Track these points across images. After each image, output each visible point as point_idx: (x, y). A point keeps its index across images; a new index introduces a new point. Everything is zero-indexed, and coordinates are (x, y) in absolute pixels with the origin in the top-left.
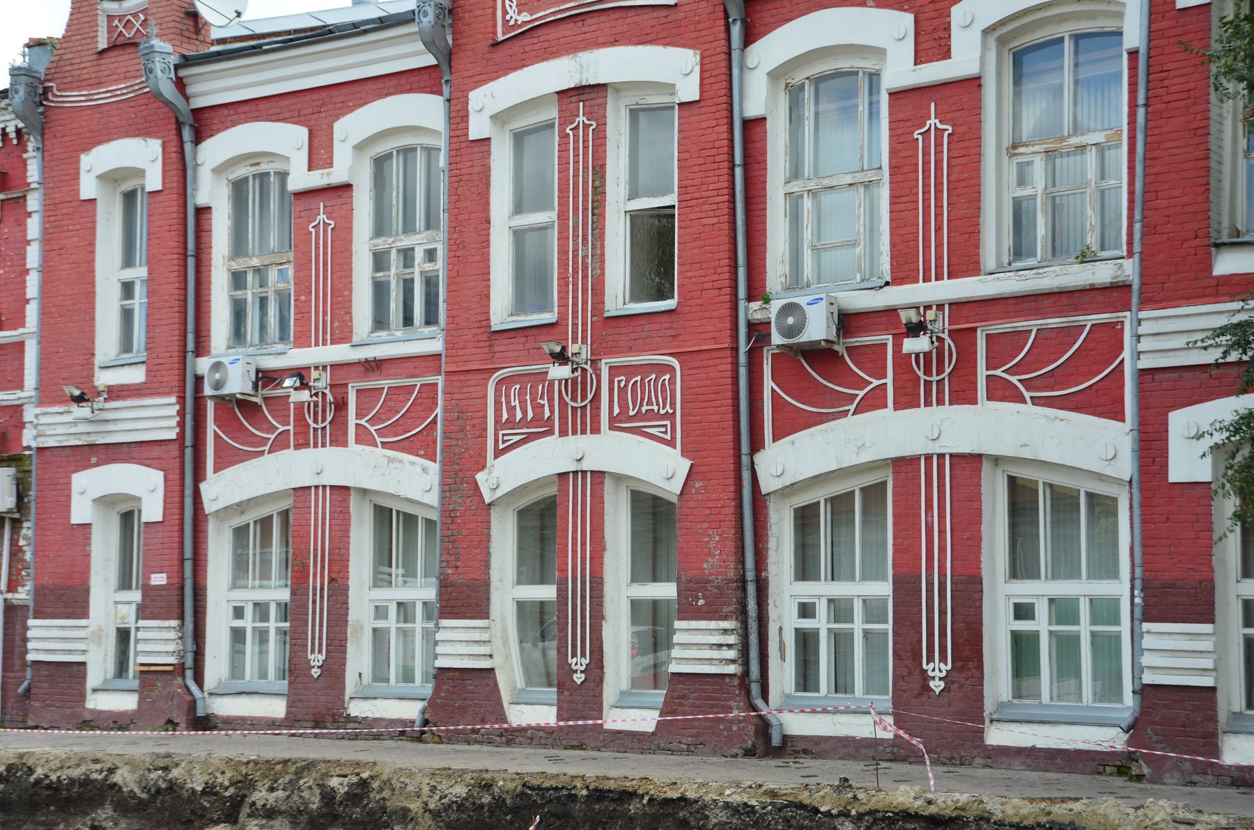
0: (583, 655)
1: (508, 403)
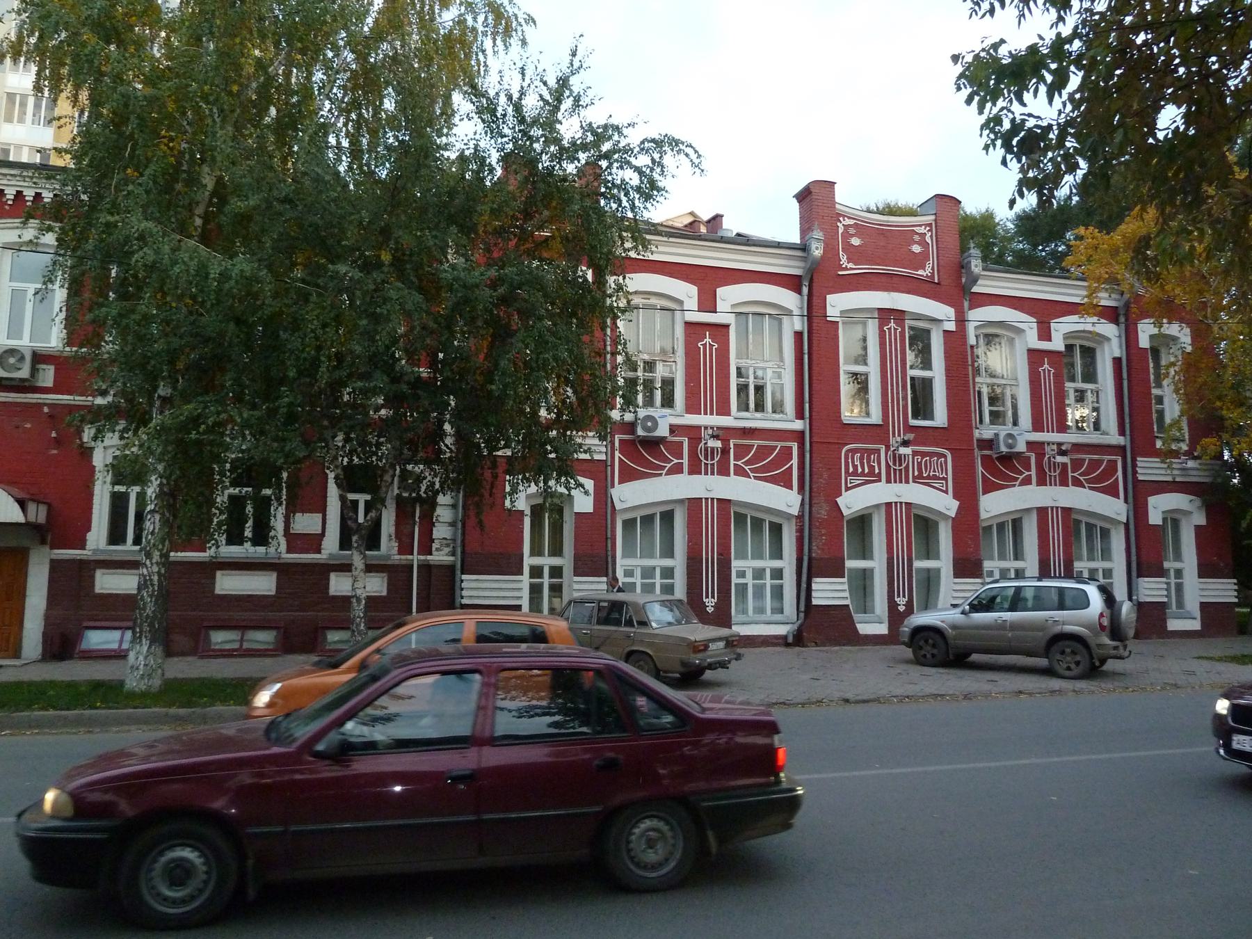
0: (904, 596)
1: (853, 462)
